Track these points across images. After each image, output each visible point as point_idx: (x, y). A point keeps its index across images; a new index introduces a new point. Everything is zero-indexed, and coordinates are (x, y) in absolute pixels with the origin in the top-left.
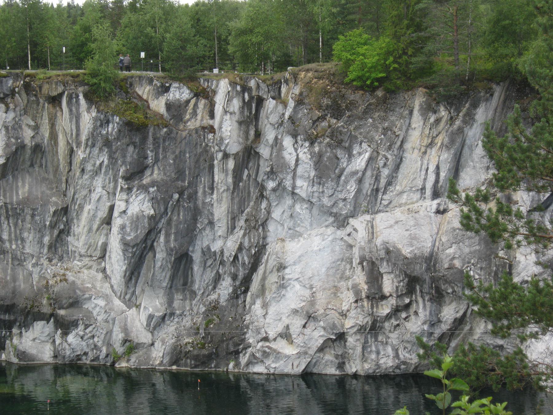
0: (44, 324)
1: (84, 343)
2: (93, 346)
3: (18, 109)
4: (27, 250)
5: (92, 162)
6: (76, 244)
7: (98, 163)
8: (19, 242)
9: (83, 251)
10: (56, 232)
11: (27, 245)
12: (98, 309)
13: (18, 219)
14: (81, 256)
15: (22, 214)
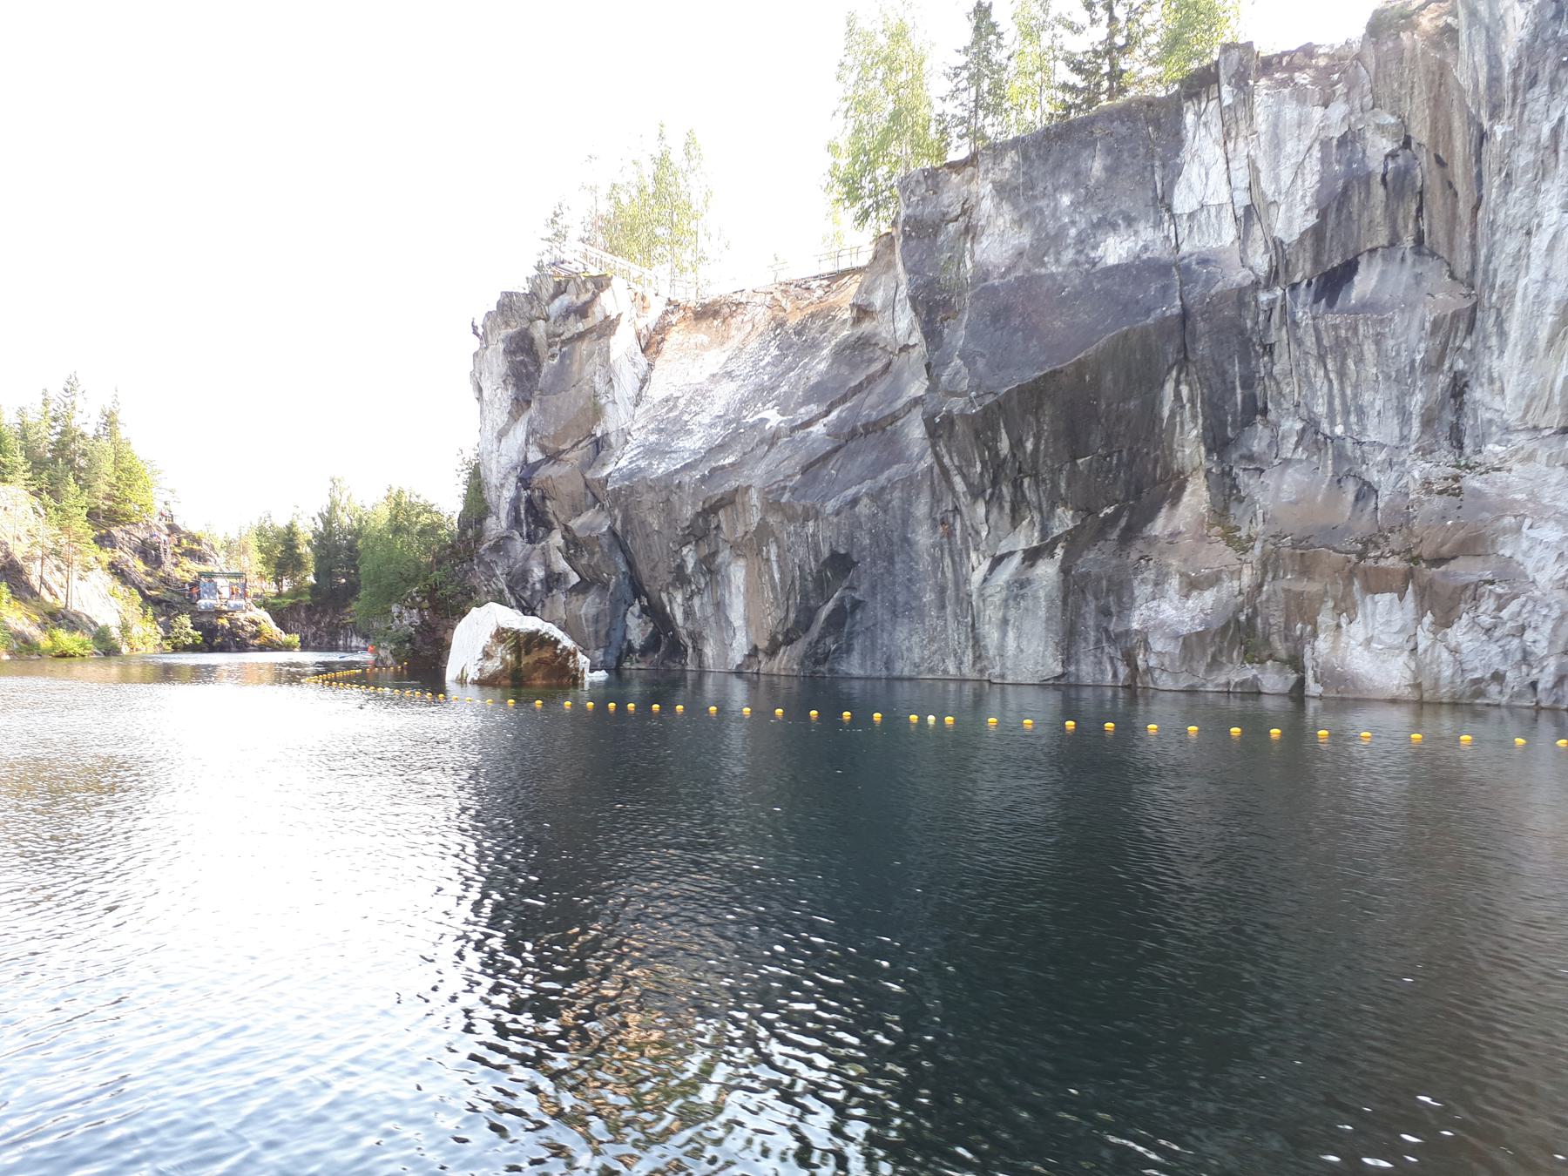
0: (1391, 601)
1: (1494, 649)
2: (1518, 656)
3: (1355, 94)
4: (1372, 435)
5: (1529, 137)
6: (1497, 403)
7: (1546, 130)
8: (1353, 418)
9: (1512, 418)
10: (1443, 380)
11: (1372, 422)
12: (1538, 552)
13: (1345, 357)
14: (1507, 429)
15: (1355, 342)
